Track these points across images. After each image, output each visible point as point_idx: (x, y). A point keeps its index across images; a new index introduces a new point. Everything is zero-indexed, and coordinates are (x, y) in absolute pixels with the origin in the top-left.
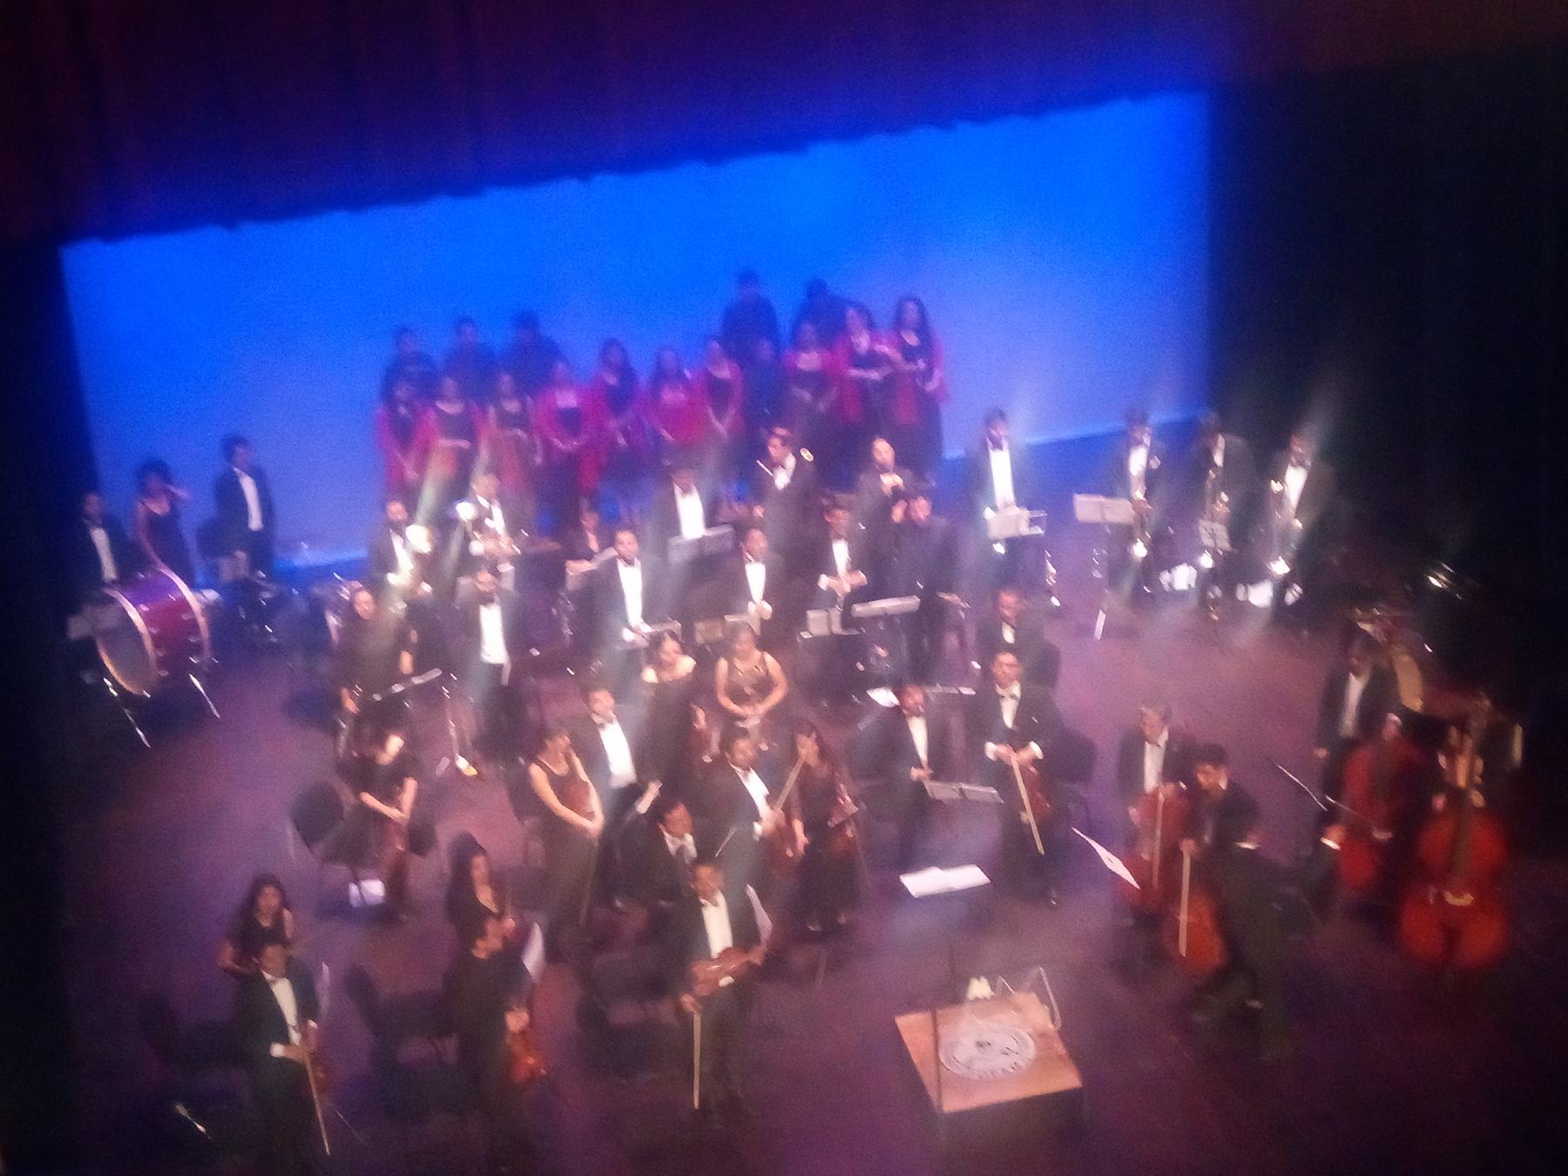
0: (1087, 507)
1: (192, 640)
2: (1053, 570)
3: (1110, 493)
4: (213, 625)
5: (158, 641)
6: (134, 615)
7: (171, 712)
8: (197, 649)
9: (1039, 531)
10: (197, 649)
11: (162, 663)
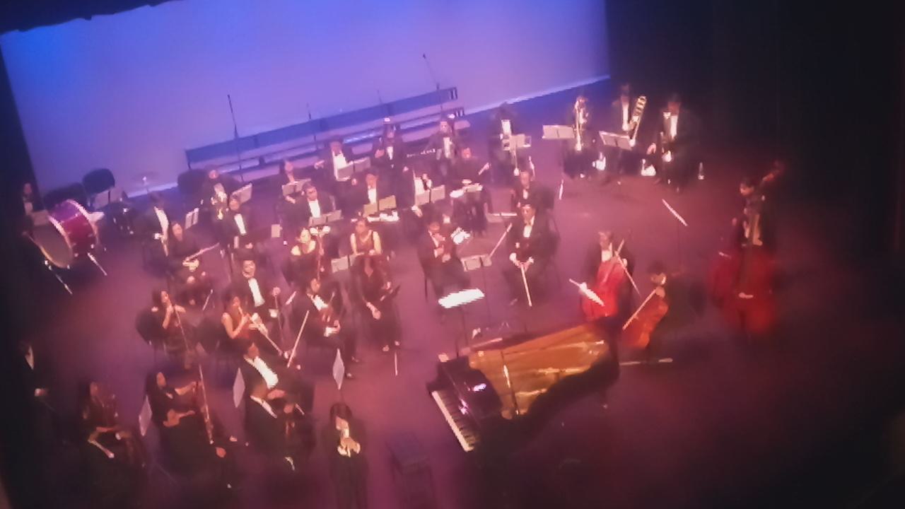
0: (551, 132)
1: (90, 235)
2: (532, 167)
3: (562, 123)
4: (99, 230)
5: (72, 238)
6: (58, 226)
7: (82, 275)
8: (93, 240)
9: (528, 146)
10: (93, 240)
11: (75, 250)
